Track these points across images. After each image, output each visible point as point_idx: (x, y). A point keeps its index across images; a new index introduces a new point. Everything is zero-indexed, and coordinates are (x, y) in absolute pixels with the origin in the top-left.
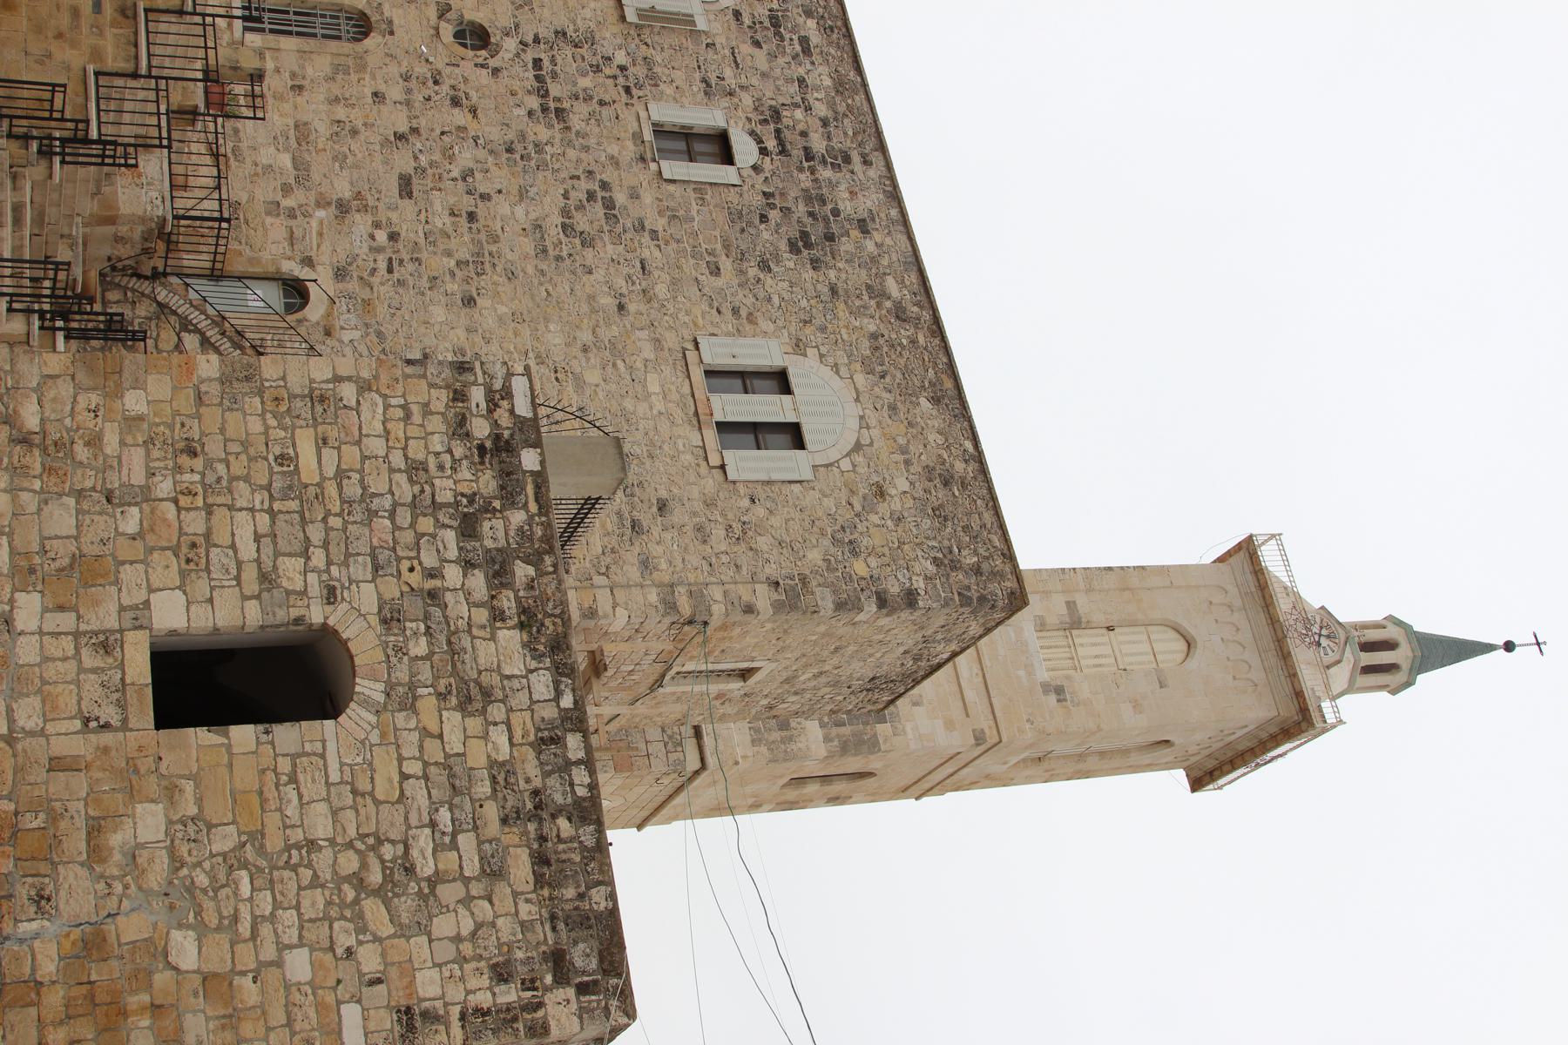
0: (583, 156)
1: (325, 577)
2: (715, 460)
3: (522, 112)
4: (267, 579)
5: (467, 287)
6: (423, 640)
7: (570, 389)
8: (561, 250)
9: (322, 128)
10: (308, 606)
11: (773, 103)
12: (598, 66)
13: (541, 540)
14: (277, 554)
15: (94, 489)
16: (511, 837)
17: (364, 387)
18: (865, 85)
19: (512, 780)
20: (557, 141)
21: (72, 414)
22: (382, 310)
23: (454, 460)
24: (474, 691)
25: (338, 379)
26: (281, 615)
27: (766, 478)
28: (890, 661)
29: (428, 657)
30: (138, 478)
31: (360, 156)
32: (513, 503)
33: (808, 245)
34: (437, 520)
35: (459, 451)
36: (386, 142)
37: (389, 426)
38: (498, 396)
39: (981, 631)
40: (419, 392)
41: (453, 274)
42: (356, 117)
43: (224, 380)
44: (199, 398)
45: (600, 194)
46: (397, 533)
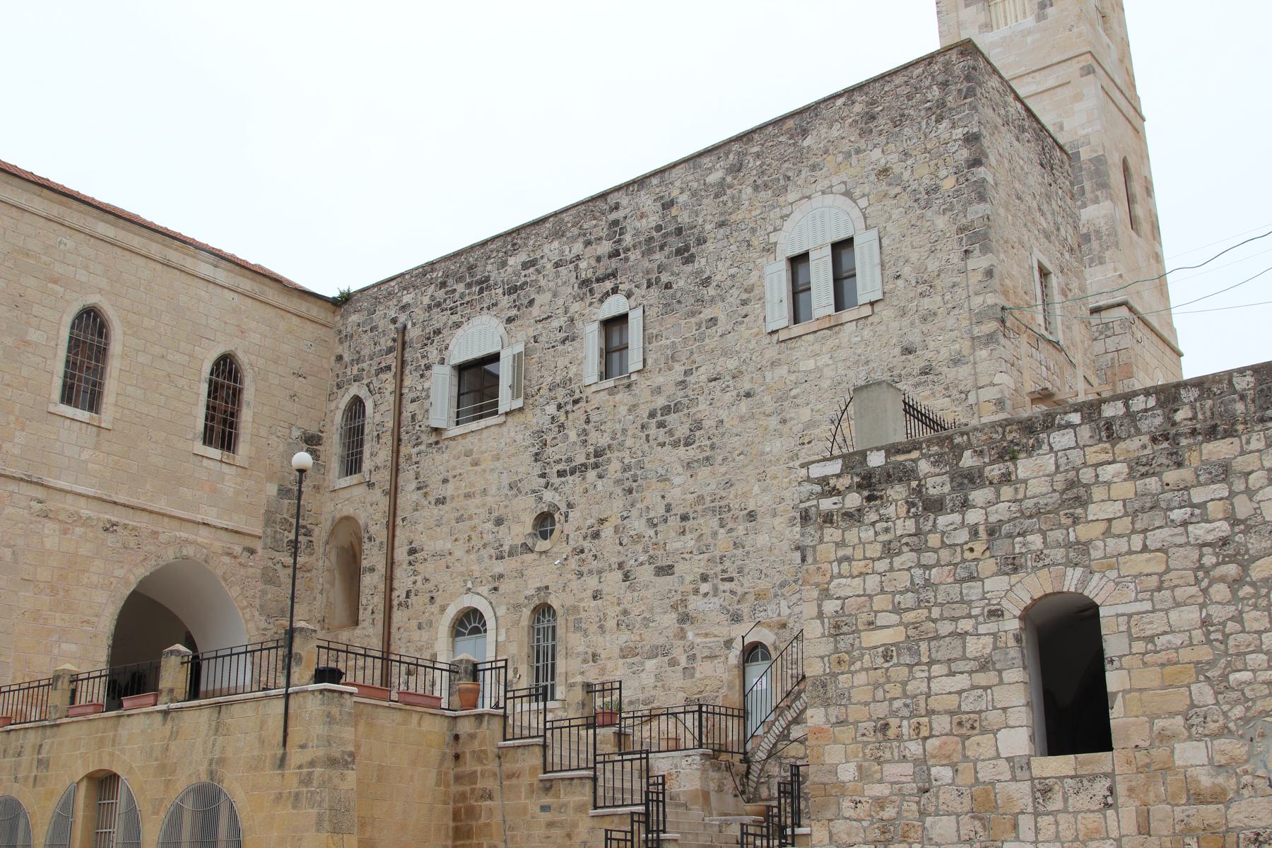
0: (630, 433)
1: (981, 619)
2: (867, 311)
3: (599, 483)
4: (985, 665)
5: (740, 518)
6: (1029, 538)
7: (816, 431)
8: (705, 446)
9: (624, 637)
10: (1006, 632)
11: (576, 286)
12: (559, 426)
13: (942, 447)
14: (964, 658)
15: (918, 803)
16: (1193, 458)
17: (825, 594)
18: (555, 214)
19: (1144, 460)
20: (620, 455)
21: (859, 820)
22: (763, 584)
23: (881, 520)
24: (1070, 494)
25: (820, 615)
26: (1014, 653)
27: (879, 267)
28: (1026, 152)
29: (1043, 533)
30: (908, 768)
31: (643, 608)
32: (912, 471)
33: (687, 248)
34: (930, 531)
35: (873, 517)
36: (632, 588)
37: (856, 573)
38: (827, 487)
39: (995, 77)
40: (827, 551)
41: (731, 530)
42: (612, 612)
43: (826, 704)
44: (840, 723)
45: (659, 418)
46: (942, 563)
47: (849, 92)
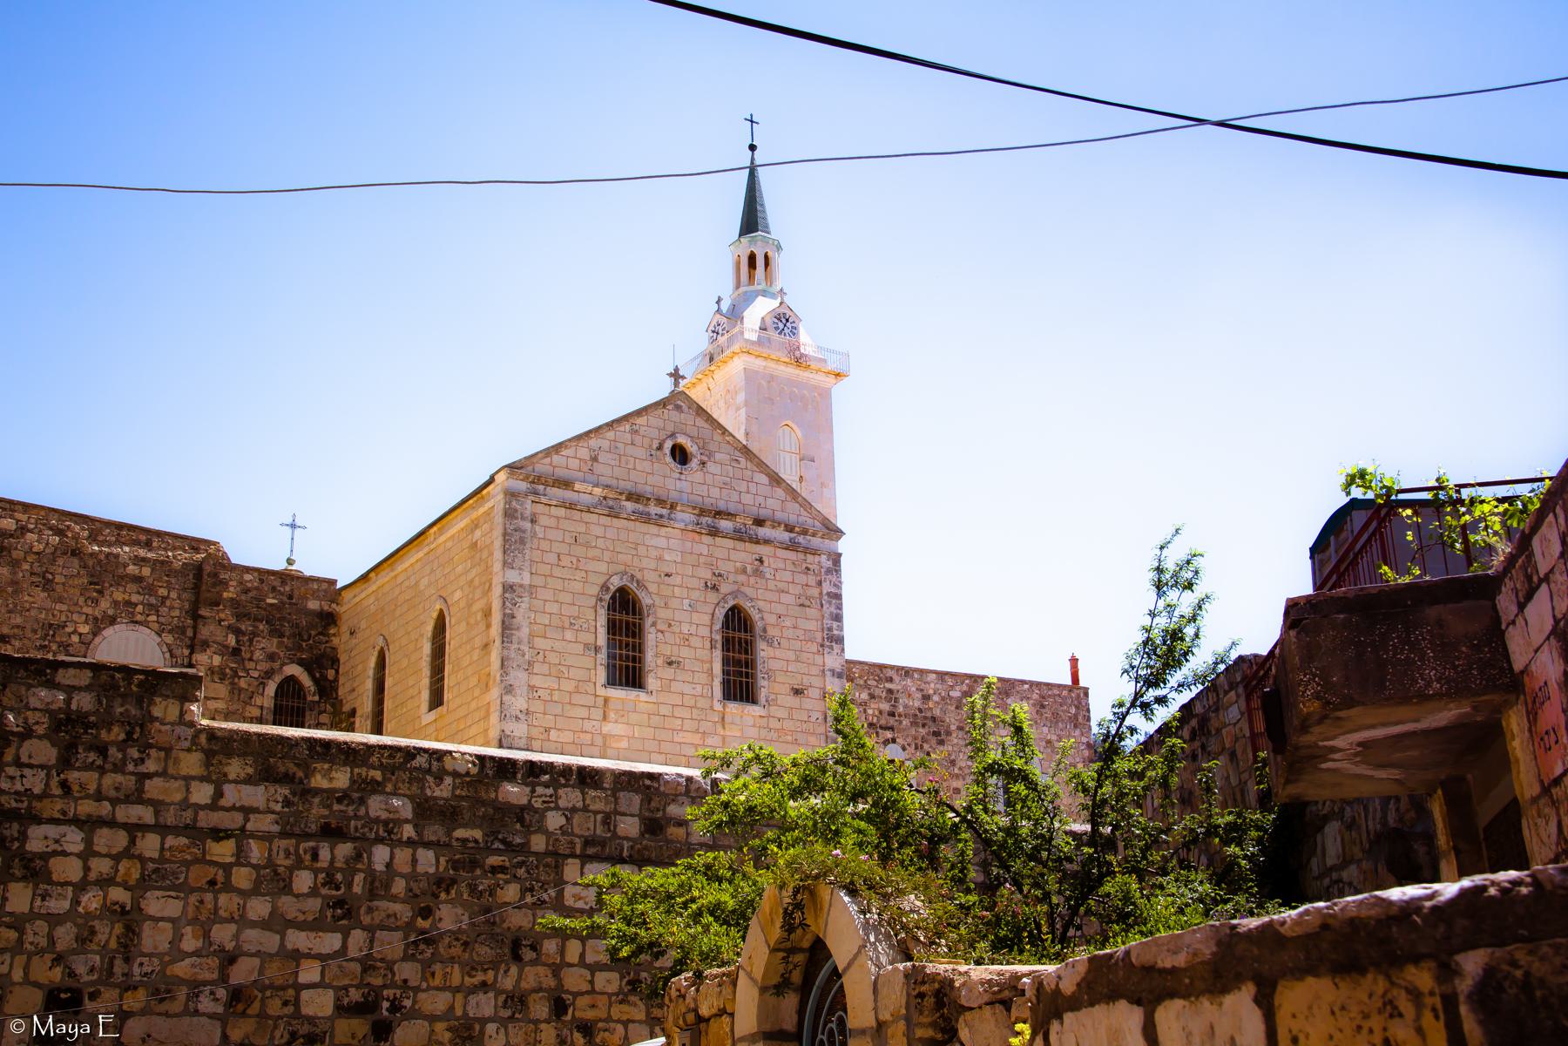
47: (1032, 684)
